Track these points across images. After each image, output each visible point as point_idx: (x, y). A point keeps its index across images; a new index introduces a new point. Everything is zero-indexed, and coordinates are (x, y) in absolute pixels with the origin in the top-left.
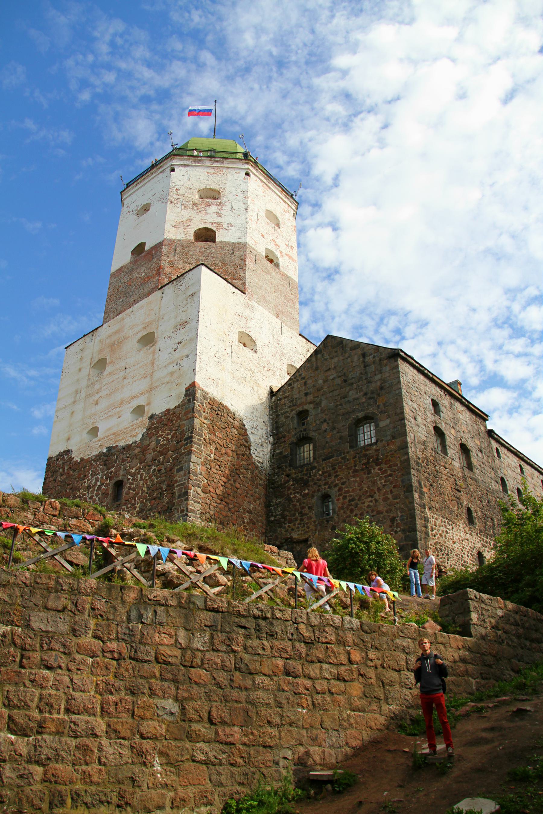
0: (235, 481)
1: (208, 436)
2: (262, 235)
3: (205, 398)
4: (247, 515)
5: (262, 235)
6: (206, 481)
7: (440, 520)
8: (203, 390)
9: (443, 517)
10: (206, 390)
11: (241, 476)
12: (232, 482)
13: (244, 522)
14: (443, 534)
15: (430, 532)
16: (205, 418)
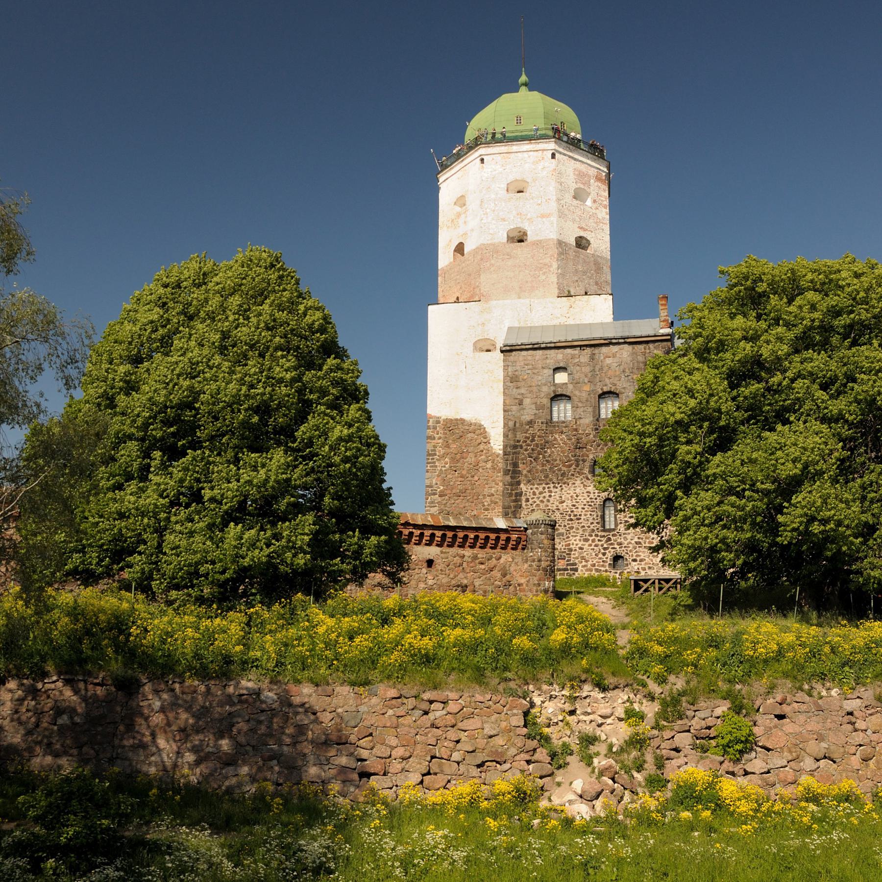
0: (473, 477)
1: (442, 452)
2: (504, 220)
3: (438, 422)
4: (488, 499)
5: (504, 220)
6: (442, 488)
7: (541, 489)
8: (435, 417)
9: (547, 484)
10: (438, 415)
11: (480, 470)
12: (470, 478)
13: (484, 506)
14: (545, 500)
15: (524, 504)
16: (440, 438)
